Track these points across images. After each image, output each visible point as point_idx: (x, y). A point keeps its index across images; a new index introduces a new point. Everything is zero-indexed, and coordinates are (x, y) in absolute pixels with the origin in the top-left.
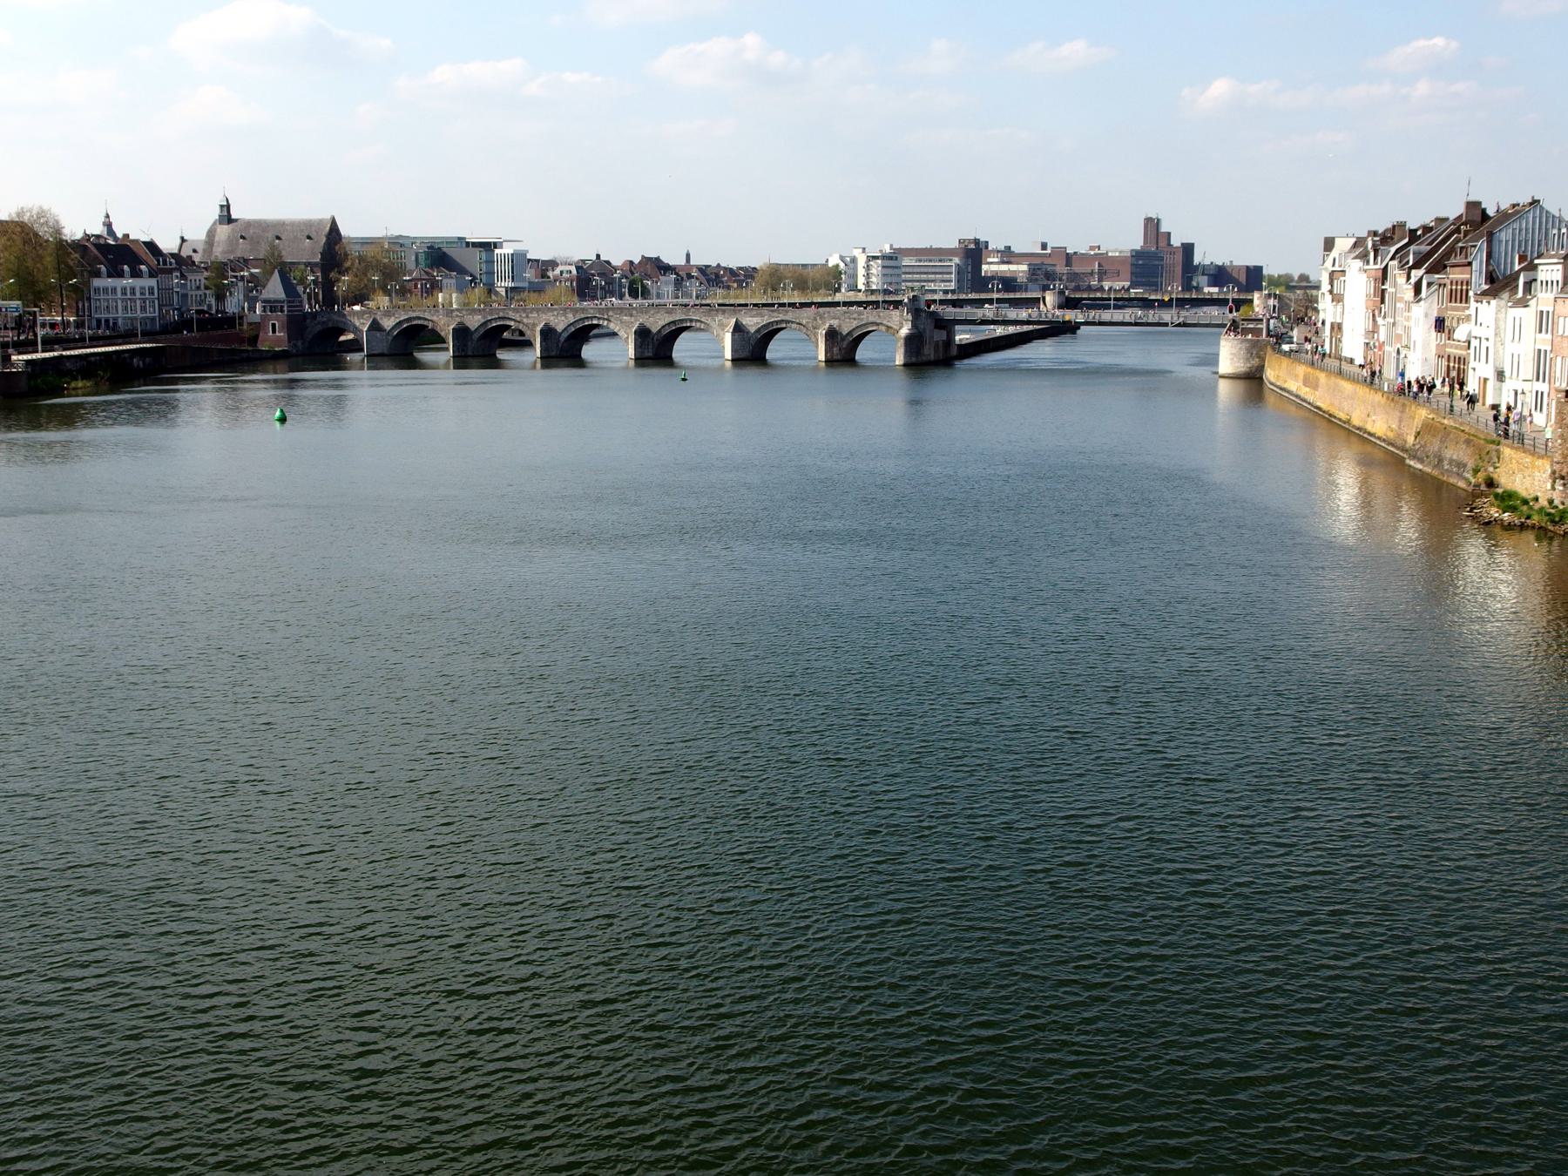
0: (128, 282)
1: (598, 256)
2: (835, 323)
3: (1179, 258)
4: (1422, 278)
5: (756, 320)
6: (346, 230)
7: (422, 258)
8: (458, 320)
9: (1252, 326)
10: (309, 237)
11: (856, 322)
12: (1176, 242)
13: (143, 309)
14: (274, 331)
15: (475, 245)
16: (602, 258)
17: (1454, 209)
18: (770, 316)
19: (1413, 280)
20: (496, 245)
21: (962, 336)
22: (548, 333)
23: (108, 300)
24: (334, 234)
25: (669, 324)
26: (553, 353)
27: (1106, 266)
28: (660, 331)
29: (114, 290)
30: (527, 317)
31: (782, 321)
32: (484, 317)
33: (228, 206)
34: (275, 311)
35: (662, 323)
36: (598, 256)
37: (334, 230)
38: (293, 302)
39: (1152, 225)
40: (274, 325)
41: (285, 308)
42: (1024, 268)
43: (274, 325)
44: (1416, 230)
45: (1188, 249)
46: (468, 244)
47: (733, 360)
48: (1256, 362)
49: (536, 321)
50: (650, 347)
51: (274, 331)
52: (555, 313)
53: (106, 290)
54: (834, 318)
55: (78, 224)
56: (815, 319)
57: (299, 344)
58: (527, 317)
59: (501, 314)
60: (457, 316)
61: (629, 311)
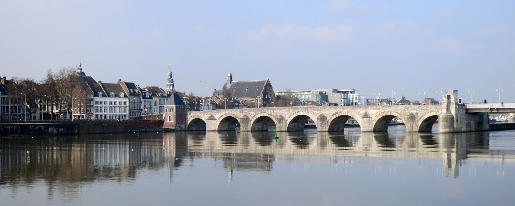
0: (113, 100)
1: (403, 98)
2: (414, 112)
5: (375, 111)
8: (245, 114)
11: (425, 111)
14: (170, 120)
18: (383, 110)
24: (268, 87)
25: (335, 114)
28: (331, 118)
29: (105, 103)
30: (273, 112)
31: (389, 111)
32: (256, 113)
34: (170, 112)
35: (331, 114)
36: (403, 98)
38: (180, 107)
40: (170, 117)
41: (174, 110)
43: (170, 117)
46: (340, 92)
49: (277, 114)
50: (327, 126)
51: (170, 120)
52: (285, 110)
53: (101, 103)
54: (414, 109)
56: (404, 110)
58: (273, 112)
60: (245, 112)
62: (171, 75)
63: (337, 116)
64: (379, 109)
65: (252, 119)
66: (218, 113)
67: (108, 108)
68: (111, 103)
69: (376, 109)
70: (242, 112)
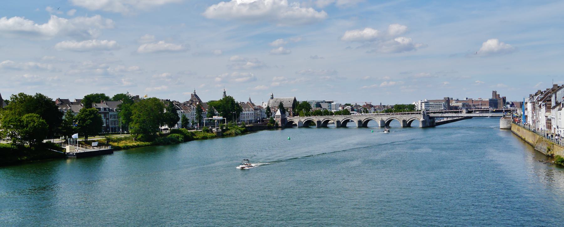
3: (502, 100)
4: (541, 104)
5: (386, 118)
6: (297, 100)
7: (315, 105)
9: (508, 116)
10: (289, 102)
12: (501, 96)
13: (247, 118)
15: (327, 102)
16: (357, 104)
17: (551, 87)
19: (539, 104)
20: (332, 102)
21: (437, 121)
22: (338, 122)
23: (242, 116)
25: (366, 119)
26: (340, 126)
27: (483, 103)
29: (245, 114)
33: (273, 95)
36: (356, 104)
37: (295, 100)
39: (494, 93)
40: (278, 121)
42: (461, 104)
43: (278, 121)
44: (543, 92)
45: (504, 99)
46: (326, 102)
47: (381, 127)
48: (509, 125)
54: (405, 117)
55: (106, 95)
56: (400, 117)
57: (284, 125)
59: (328, 118)
61: (357, 116)
62: (225, 93)
63: (367, 119)
64: (388, 117)
65: (322, 121)
66: (303, 118)
67: (246, 118)
68: (247, 114)
69: (386, 117)
70: (316, 118)
